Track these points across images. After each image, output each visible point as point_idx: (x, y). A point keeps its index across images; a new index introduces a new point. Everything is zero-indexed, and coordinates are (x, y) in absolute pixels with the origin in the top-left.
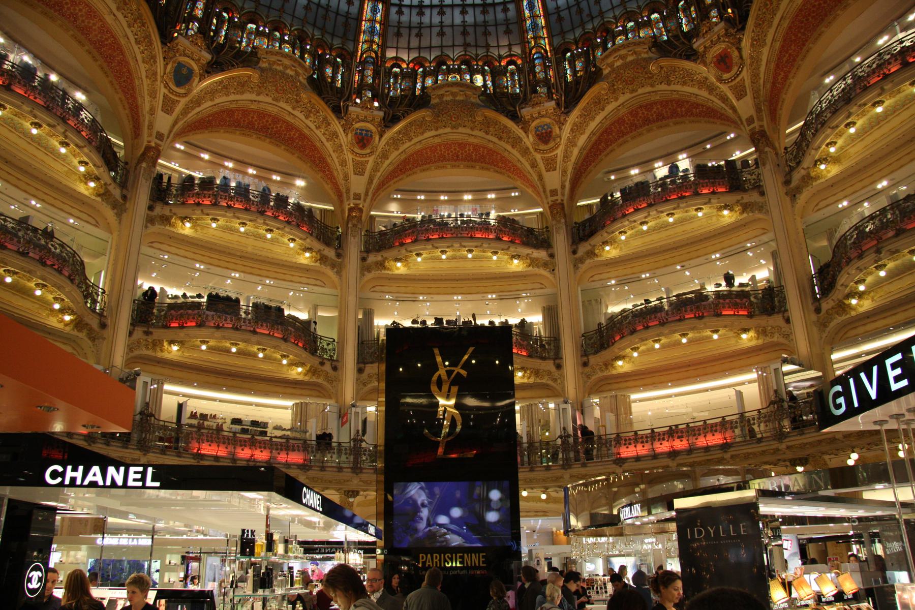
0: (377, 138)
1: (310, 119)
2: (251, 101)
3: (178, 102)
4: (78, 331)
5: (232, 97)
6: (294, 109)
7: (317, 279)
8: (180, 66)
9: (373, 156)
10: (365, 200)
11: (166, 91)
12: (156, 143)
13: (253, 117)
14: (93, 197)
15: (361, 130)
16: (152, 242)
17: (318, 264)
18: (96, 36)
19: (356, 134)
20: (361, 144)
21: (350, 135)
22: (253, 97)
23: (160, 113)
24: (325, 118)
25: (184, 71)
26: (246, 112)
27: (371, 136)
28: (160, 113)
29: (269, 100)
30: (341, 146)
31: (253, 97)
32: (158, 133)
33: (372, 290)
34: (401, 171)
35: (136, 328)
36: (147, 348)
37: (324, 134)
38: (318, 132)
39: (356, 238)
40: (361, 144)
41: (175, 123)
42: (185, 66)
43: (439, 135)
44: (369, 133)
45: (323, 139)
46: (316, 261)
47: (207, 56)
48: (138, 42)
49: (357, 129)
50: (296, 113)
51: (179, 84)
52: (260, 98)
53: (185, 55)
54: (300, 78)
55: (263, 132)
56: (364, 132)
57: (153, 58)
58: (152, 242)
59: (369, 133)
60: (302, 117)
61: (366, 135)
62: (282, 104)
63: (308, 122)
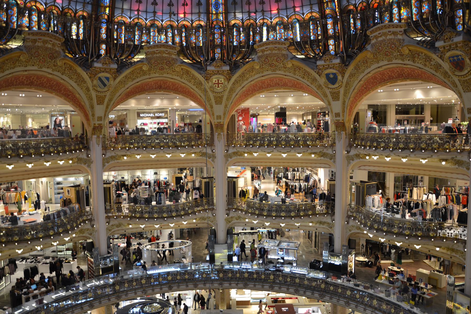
1: (417, 62)
2: (377, 68)
3: (339, 92)
6: (403, 60)
7: (464, 175)
8: (327, 75)
11: (330, 90)
13: (388, 73)
15: (453, 57)
16: (360, 167)
17: (457, 166)
19: (450, 61)
21: (447, 64)
23: (333, 103)
25: (331, 76)
28: (333, 103)
29: (386, 62)
32: (336, 114)
37: (431, 68)
38: (427, 68)
41: (344, 103)
44: (460, 57)
46: (455, 165)
48: (303, 78)
49: (450, 57)
51: (333, 83)
55: (401, 77)
56: (455, 58)
57: (314, 80)
58: (360, 167)
61: (459, 59)
63: (416, 64)
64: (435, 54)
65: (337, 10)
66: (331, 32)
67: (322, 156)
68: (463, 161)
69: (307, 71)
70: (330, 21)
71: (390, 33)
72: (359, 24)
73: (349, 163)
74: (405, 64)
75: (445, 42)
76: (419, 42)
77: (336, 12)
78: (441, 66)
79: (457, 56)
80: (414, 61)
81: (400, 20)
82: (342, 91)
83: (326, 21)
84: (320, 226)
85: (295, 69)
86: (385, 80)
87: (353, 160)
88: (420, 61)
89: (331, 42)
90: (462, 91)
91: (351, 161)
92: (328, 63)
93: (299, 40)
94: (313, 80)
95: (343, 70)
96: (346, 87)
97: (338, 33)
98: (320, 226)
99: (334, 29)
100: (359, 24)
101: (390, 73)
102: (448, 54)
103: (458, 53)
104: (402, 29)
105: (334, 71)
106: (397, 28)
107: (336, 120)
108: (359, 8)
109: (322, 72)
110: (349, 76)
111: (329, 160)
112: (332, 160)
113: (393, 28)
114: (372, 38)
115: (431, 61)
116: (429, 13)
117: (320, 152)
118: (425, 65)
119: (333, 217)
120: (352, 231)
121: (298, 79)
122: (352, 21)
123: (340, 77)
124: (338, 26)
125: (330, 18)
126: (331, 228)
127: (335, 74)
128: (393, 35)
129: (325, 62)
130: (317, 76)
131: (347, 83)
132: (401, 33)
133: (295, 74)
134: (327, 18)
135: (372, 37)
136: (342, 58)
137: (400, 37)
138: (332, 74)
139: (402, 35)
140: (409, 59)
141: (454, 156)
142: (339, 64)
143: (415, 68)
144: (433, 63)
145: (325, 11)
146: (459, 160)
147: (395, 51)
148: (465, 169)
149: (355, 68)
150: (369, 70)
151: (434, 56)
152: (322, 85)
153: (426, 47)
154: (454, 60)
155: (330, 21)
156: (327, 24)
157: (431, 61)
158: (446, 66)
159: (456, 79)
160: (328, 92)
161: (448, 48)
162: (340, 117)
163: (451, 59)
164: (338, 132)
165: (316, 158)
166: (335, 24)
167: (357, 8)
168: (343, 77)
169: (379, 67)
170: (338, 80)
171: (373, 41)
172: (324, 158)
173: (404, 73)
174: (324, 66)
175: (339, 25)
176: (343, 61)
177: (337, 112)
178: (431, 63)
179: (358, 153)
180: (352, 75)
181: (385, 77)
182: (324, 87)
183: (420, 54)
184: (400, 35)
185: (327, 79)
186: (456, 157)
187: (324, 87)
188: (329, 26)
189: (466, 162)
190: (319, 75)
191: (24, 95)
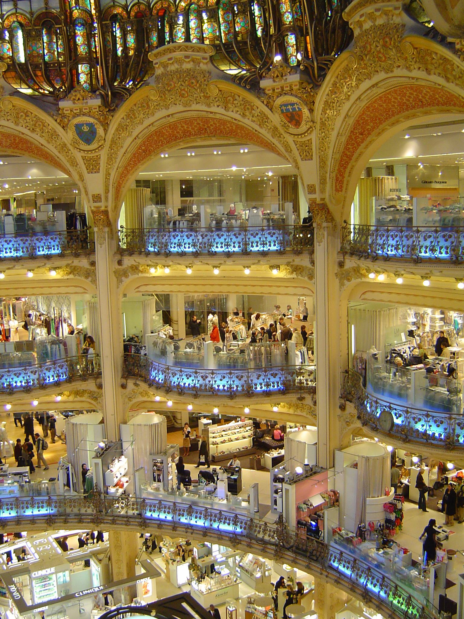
0: (305, 111)
1: (231, 110)
2: (165, 117)
3: (98, 158)
4: (80, 397)
5: (147, 123)
6: (209, 106)
7: (304, 288)
8: (78, 127)
9: (314, 132)
10: (322, 191)
11: (82, 154)
12: (95, 207)
13: (183, 127)
14: (66, 277)
15: (286, 105)
16: (138, 288)
17: (294, 276)
18: (6, 141)
19: (282, 110)
20: (294, 122)
21: (277, 115)
22: (164, 113)
24: (246, 102)
25: (86, 129)
26: (173, 126)
27: (300, 110)
29: (180, 108)
30: (276, 128)
31: (164, 113)
32: (93, 196)
33: (363, 296)
34: (361, 134)
35: (128, 381)
36: (142, 396)
38: (246, 121)
39: (322, 244)
40: (294, 122)
42: (83, 125)
43: (376, 84)
44: (296, 106)
45: (257, 128)
46: (292, 273)
47: (98, 102)
48: (33, 130)
49: (281, 106)
50: (214, 109)
51: (88, 141)
52: (170, 112)
53: (76, 116)
54: (201, 65)
55: (204, 134)
56: (289, 107)
57: (54, 135)
58: (138, 288)
59: (296, 106)
60: (221, 110)
61: (294, 109)
62: (194, 107)
63: (230, 114)
64: (259, 98)
65: (93, 12)
66: (82, 50)
67: (70, 273)
68: (303, 267)
69: (39, 119)
70: (80, 31)
71: (187, 60)
72: (131, 40)
73: (120, 281)
74: (211, 113)
75: (274, 81)
76: (233, 79)
77: (91, 16)
78: (267, 118)
79: (292, 104)
80: (226, 108)
81: (202, 39)
82: (104, 154)
83: (75, 30)
84: (76, 399)
85: (18, 114)
86: (176, 138)
87: (127, 276)
88: (237, 109)
89: (82, 68)
90: (299, 159)
91: (123, 278)
92: (79, 105)
93: (22, 60)
94: (52, 135)
95: (106, 119)
96: (111, 148)
97: (96, 52)
98: (76, 399)
99: (89, 46)
100: (132, 41)
101: (186, 126)
102: (280, 101)
103: (294, 100)
104: (207, 55)
105: (91, 120)
106: (198, 52)
107: (95, 207)
108: (133, 13)
109: (69, 121)
110: (117, 130)
111: (83, 278)
112: (90, 279)
113: (193, 51)
114: (157, 66)
115: (253, 109)
116: (247, 32)
117: (67, 265)
118: (244, 115)
119: (98, 380)
120: (134, 401)
121: (23, 134)
122: (118, 34)
123: (100, 131)
124: (95, 41)
125: (82, 25)
126: (96, 399)
127: (91, 125)
128: (192, 63)
129: (74, 103)
130: (59, 129)
131: (113, 142)
132: (205, 61)
133: (17, 124)
134: (77, 25)
135: (156, 64)
136: (104, 98)
137: (203, 66)
138: (87, 124)
139: (207, 63)
140: (218, 103)
141: (291, 260)
142: (100, 107)
143: (230, 119)
144: (256, 113)
145: (71, 13)
146: (297, 266)
147: (196, 90)
148: (306, 278)
149: (128, 116)
150: (152, 120)
151: (257, 102)
152: (69, 145)
153: (245, 87)
154: (287, 110)
155: (80, 31)
156: (75, 36)
157: (253, 109)
158: (276, 119)
159: (290, 139)
160: (78, 156)
161: (280, 90)
162: (101, 201)
163: (283, 108)
164: (99, 229)
165: (59, 277)
166: (89, 36)
167: (128, 13)
168: (106, 130)
169: (169, 116)
170: (97, 136)
171: (159, 71)
172: (75, 275)
173: (208, 127)
174: (71, 111)
175: (96, 39)
176: (105, 103)
177: (96, 192)
178: (253, 111)
179: (135, 264)
180: (122, 128)
181: (178, 132)
182: (71, 148)
183: (237, 97)
184: (204, 63)
185: (78, 134)
186: (293, 260)
187: (71, 148)
188: (80, 40)
189: (306, 267)
190: (63, 127)
191: (246, 151)
